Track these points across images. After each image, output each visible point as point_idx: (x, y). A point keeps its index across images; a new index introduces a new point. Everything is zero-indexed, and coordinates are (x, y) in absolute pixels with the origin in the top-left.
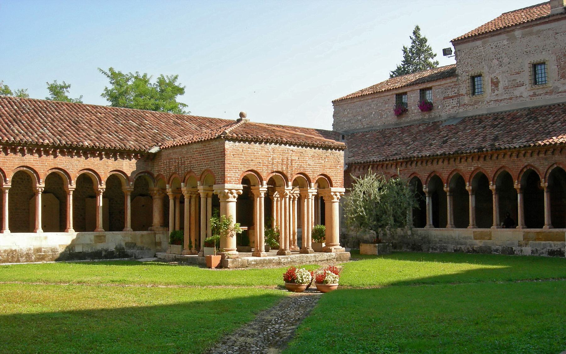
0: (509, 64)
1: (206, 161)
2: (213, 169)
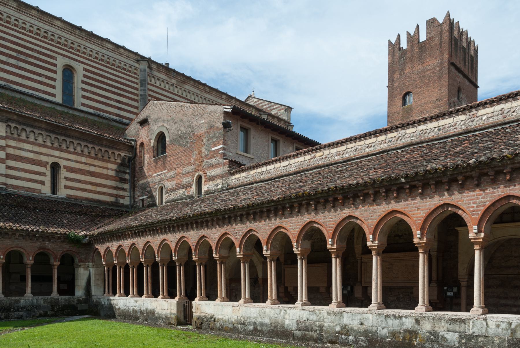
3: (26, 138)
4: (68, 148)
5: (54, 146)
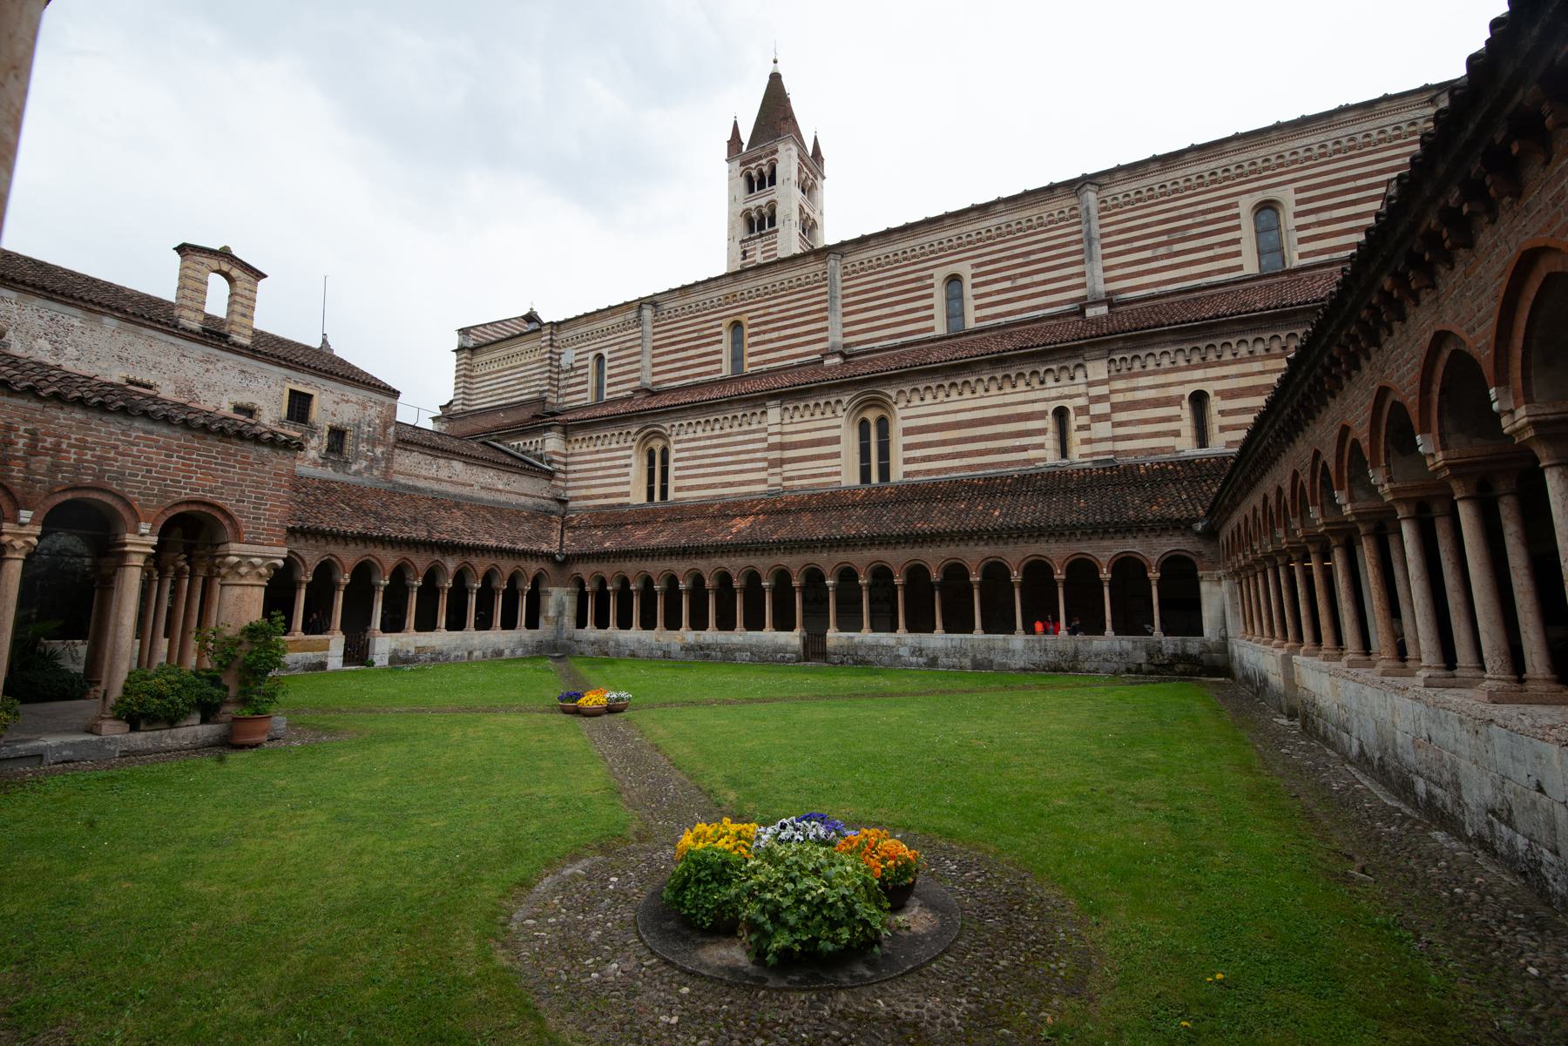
0: (78, 360)
1: (197, 479)
2: (231, 505)
3: (1141, 370)
4: (1219, 357)
5: (1192, 363)
